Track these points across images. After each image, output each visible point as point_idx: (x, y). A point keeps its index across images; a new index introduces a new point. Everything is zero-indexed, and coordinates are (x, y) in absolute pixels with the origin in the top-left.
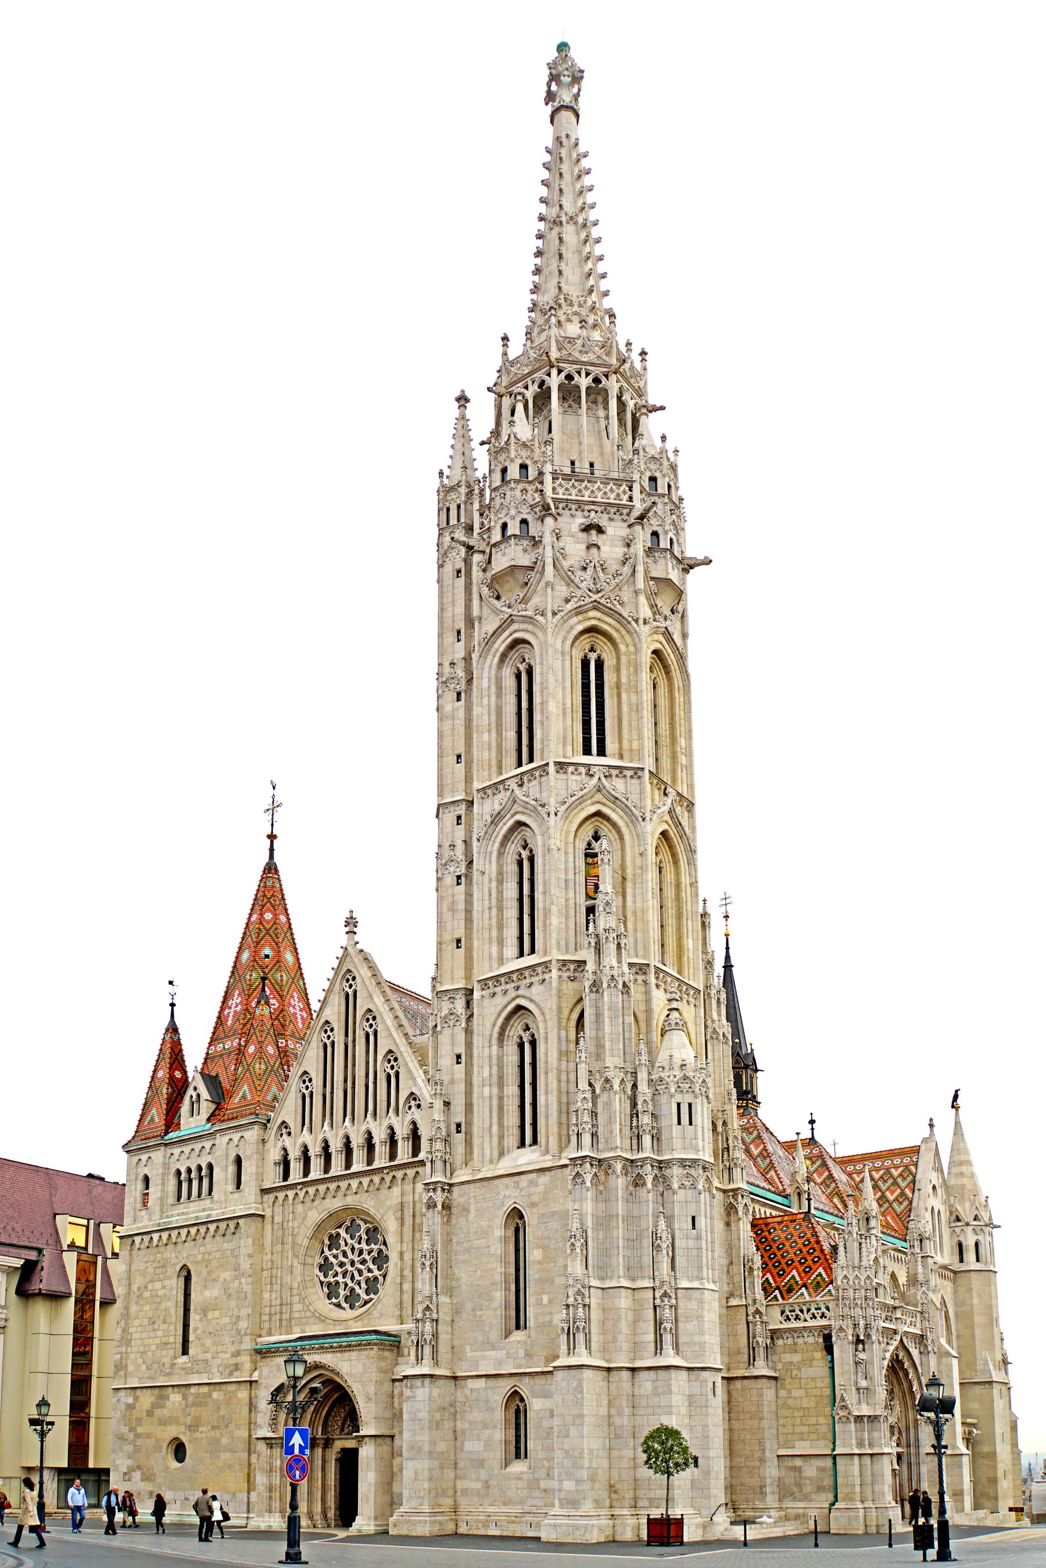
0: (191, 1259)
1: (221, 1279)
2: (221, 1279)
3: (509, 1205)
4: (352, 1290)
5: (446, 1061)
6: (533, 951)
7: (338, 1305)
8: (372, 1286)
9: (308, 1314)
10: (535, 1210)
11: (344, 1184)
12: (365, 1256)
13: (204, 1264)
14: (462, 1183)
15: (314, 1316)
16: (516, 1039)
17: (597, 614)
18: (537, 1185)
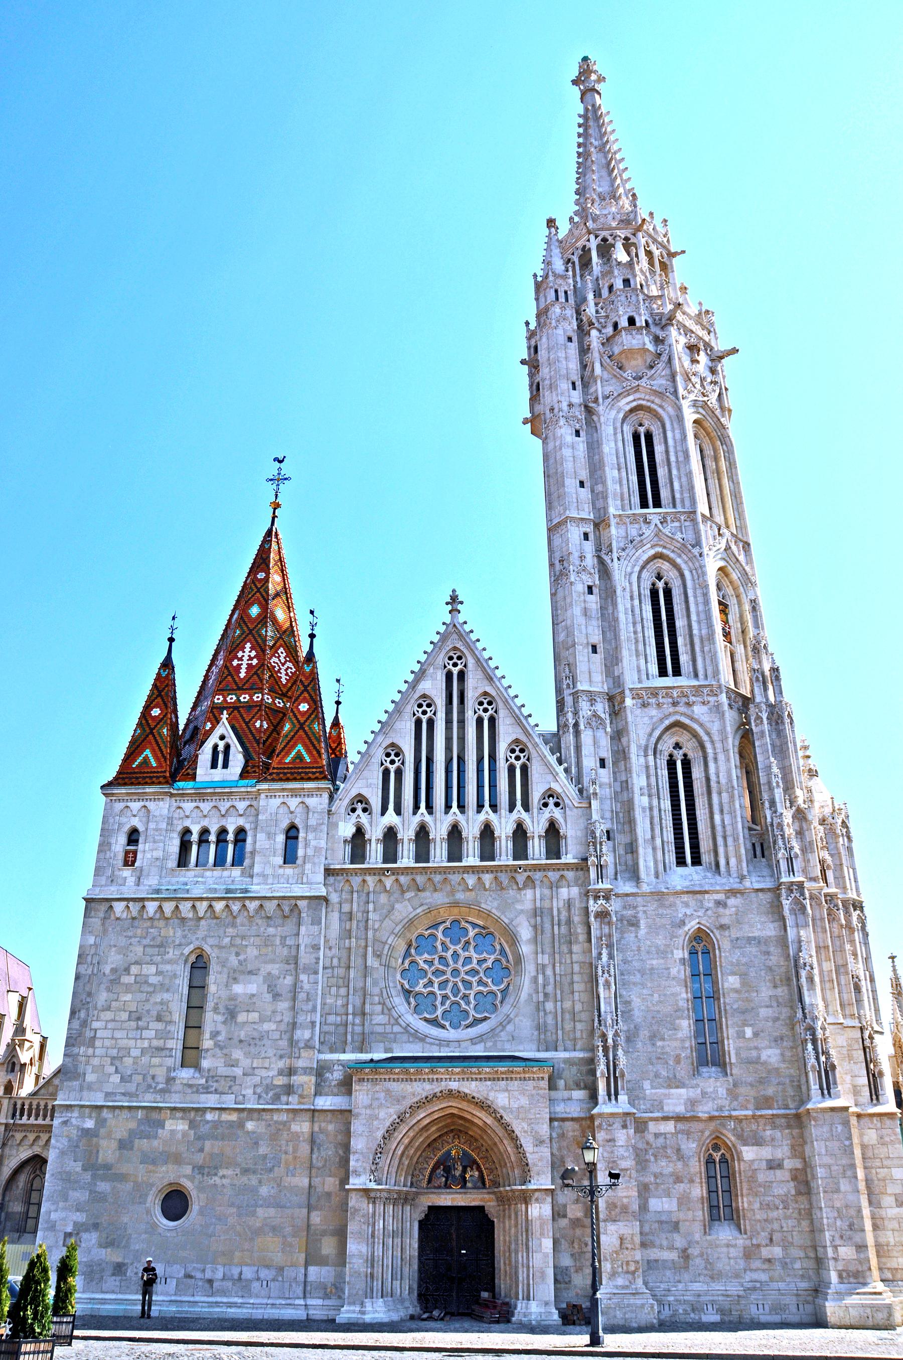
0: (211, 941)
1: (263, 972)
2: (263, 972)
3: (692, 926)
5: (589, 762)
6: (677, 672)
9: (396, 1029)
10: (727, 933)
11: (455, 878)
12: (474, 964)
13: (233, 950)
14: (627, 895)
15: (407, 1032)
16: (667, 754)
17: (704, 413)
18: (725, 905)
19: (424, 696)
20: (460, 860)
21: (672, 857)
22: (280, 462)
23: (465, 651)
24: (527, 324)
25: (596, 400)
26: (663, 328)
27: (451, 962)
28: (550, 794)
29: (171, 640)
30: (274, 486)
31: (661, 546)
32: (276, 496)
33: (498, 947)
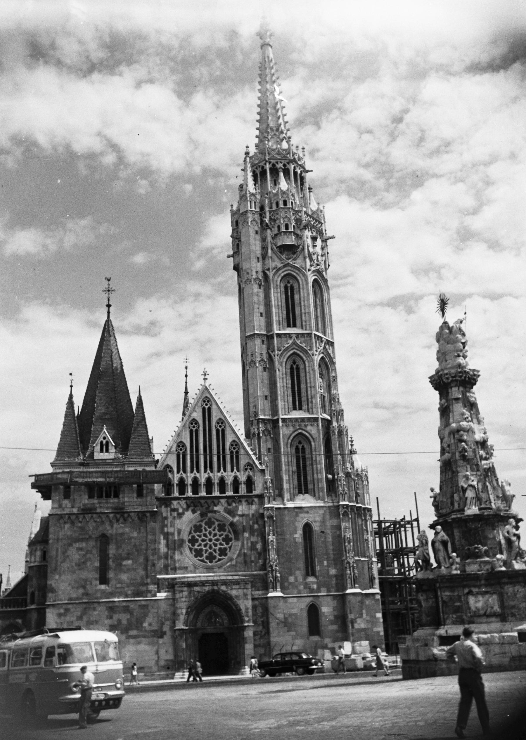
4: (211, 554)
7: (202, 561)
8: (223, 552)
11: (209, 501)
19: (194, 420)
20: (211, 494)
21: (297, 491)
22: (109, 280)
23: (211, 399)
24: (232, 206)
25: (268, 270)
26: (301, 230)
27: (208, 535)
28: (249, 464)
29: (71, 386)
30: (107, 295)
31: (296, 349)
32: (109, 300)
33: (227, 529)
